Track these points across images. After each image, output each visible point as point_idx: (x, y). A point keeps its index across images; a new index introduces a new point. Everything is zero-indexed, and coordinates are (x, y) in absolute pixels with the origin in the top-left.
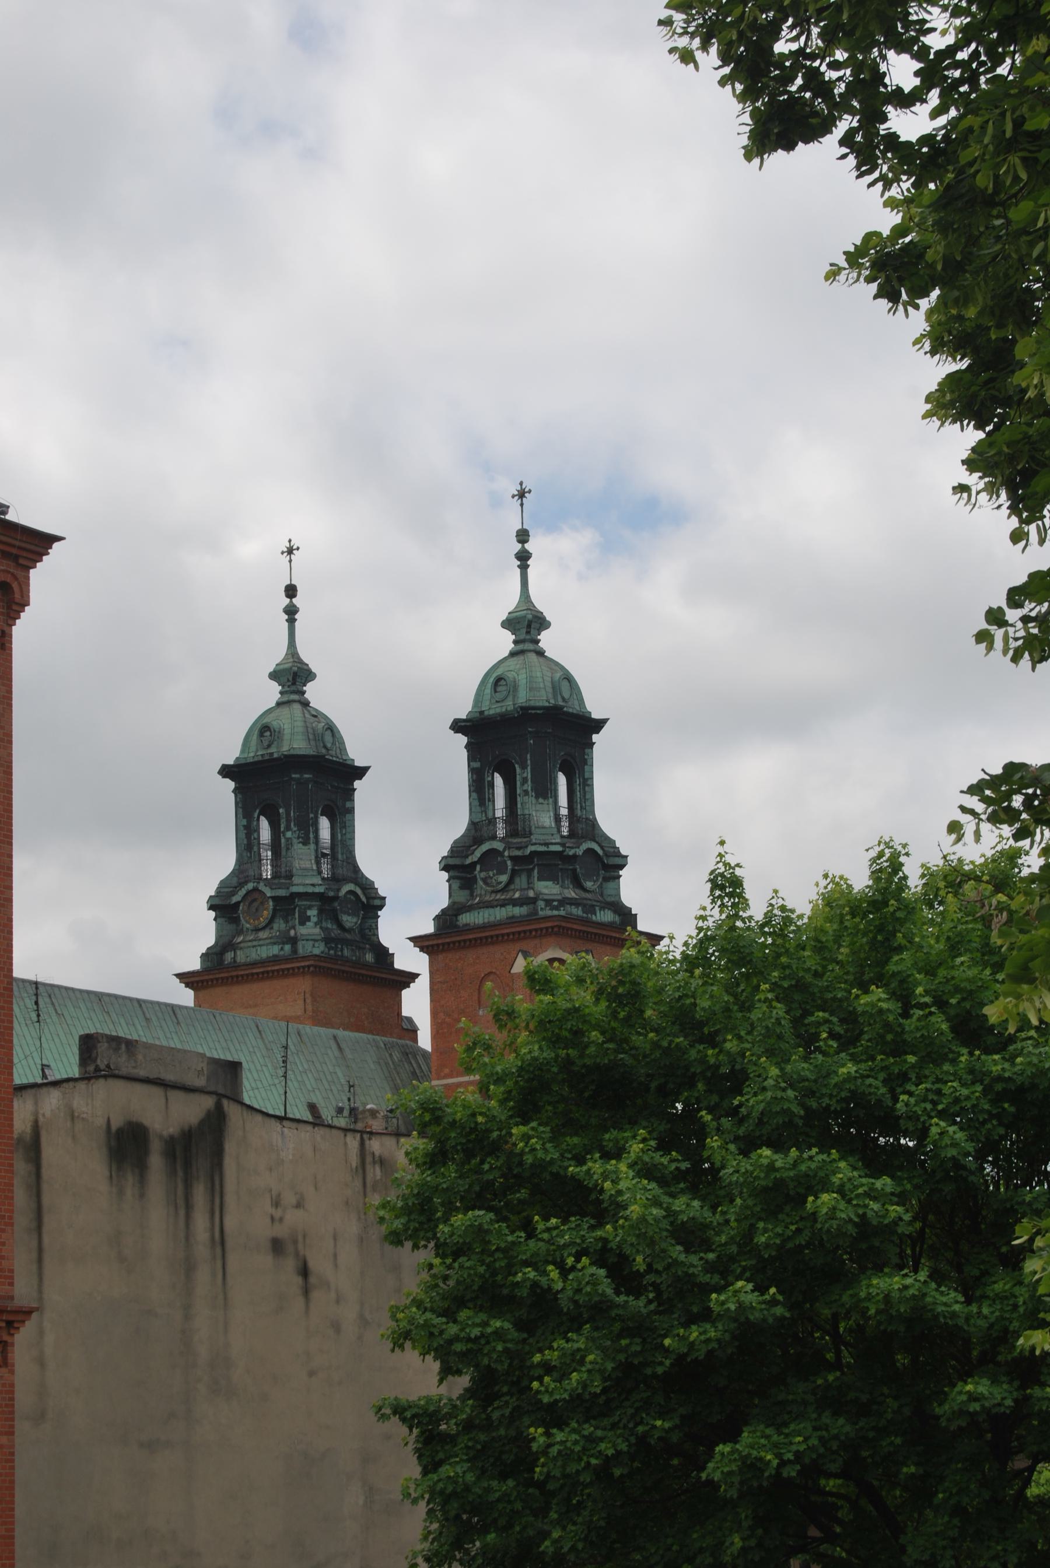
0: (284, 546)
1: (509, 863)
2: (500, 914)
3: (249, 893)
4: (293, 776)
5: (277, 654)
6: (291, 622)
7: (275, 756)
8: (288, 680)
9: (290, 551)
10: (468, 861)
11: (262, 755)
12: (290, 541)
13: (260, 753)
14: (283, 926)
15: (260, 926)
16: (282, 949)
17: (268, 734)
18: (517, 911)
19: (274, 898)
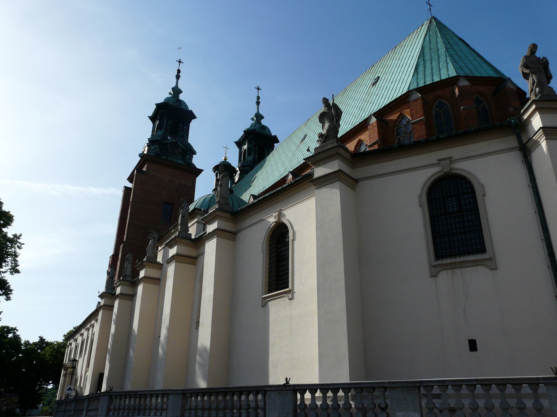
0: (178, 60)
12: (177, 61)
14: (181, 158)
15: (175, 154)
17: (179, 102)
19: (182, 148)
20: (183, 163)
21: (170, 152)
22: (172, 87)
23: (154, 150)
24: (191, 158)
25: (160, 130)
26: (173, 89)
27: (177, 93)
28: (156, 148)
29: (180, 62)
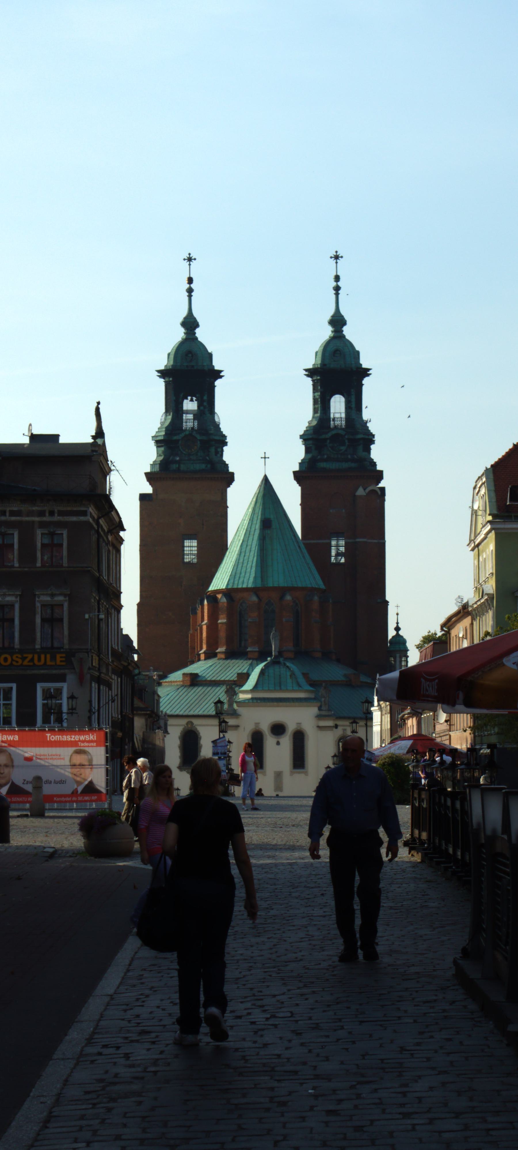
0: (186, 256)
1: (346, 441)
2: (345, 465)
3: (186, 436)
4: (208, 379)
5: (184, 313)
6: (190, 296)
7: (195, 368)
8: (191, 327)
9: (190, 259)
10: (323, 436)
11: (187, 366)
13: (185, 364)
16: (206, 466)
17: (190, 355)
18: (353, 465)
19: (200, 440)
20: (203, 466)
21: (184, 452)
22: (181, 319)
23: (162, 456)
24: (219, 450)
25: (168, 414)
26: (184, 324)
27: (191, 327)
28: (164, 452)
29: (190, 259)
